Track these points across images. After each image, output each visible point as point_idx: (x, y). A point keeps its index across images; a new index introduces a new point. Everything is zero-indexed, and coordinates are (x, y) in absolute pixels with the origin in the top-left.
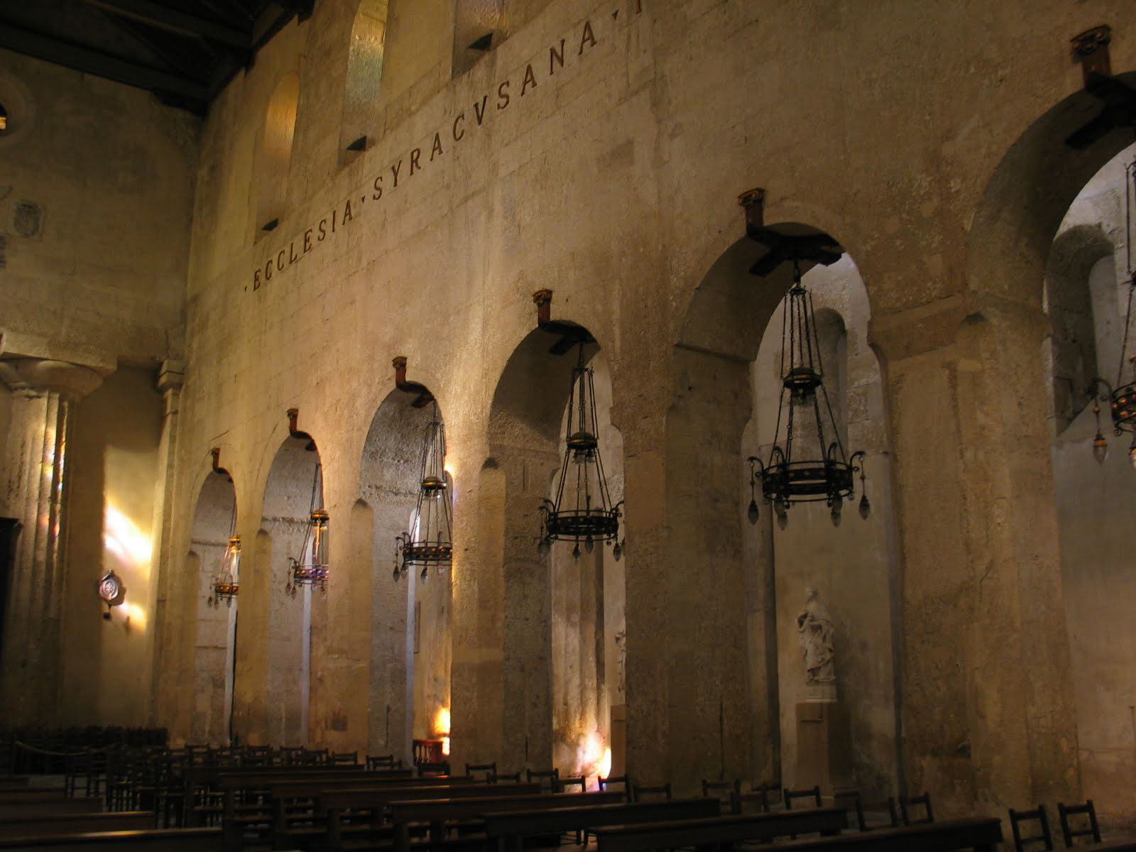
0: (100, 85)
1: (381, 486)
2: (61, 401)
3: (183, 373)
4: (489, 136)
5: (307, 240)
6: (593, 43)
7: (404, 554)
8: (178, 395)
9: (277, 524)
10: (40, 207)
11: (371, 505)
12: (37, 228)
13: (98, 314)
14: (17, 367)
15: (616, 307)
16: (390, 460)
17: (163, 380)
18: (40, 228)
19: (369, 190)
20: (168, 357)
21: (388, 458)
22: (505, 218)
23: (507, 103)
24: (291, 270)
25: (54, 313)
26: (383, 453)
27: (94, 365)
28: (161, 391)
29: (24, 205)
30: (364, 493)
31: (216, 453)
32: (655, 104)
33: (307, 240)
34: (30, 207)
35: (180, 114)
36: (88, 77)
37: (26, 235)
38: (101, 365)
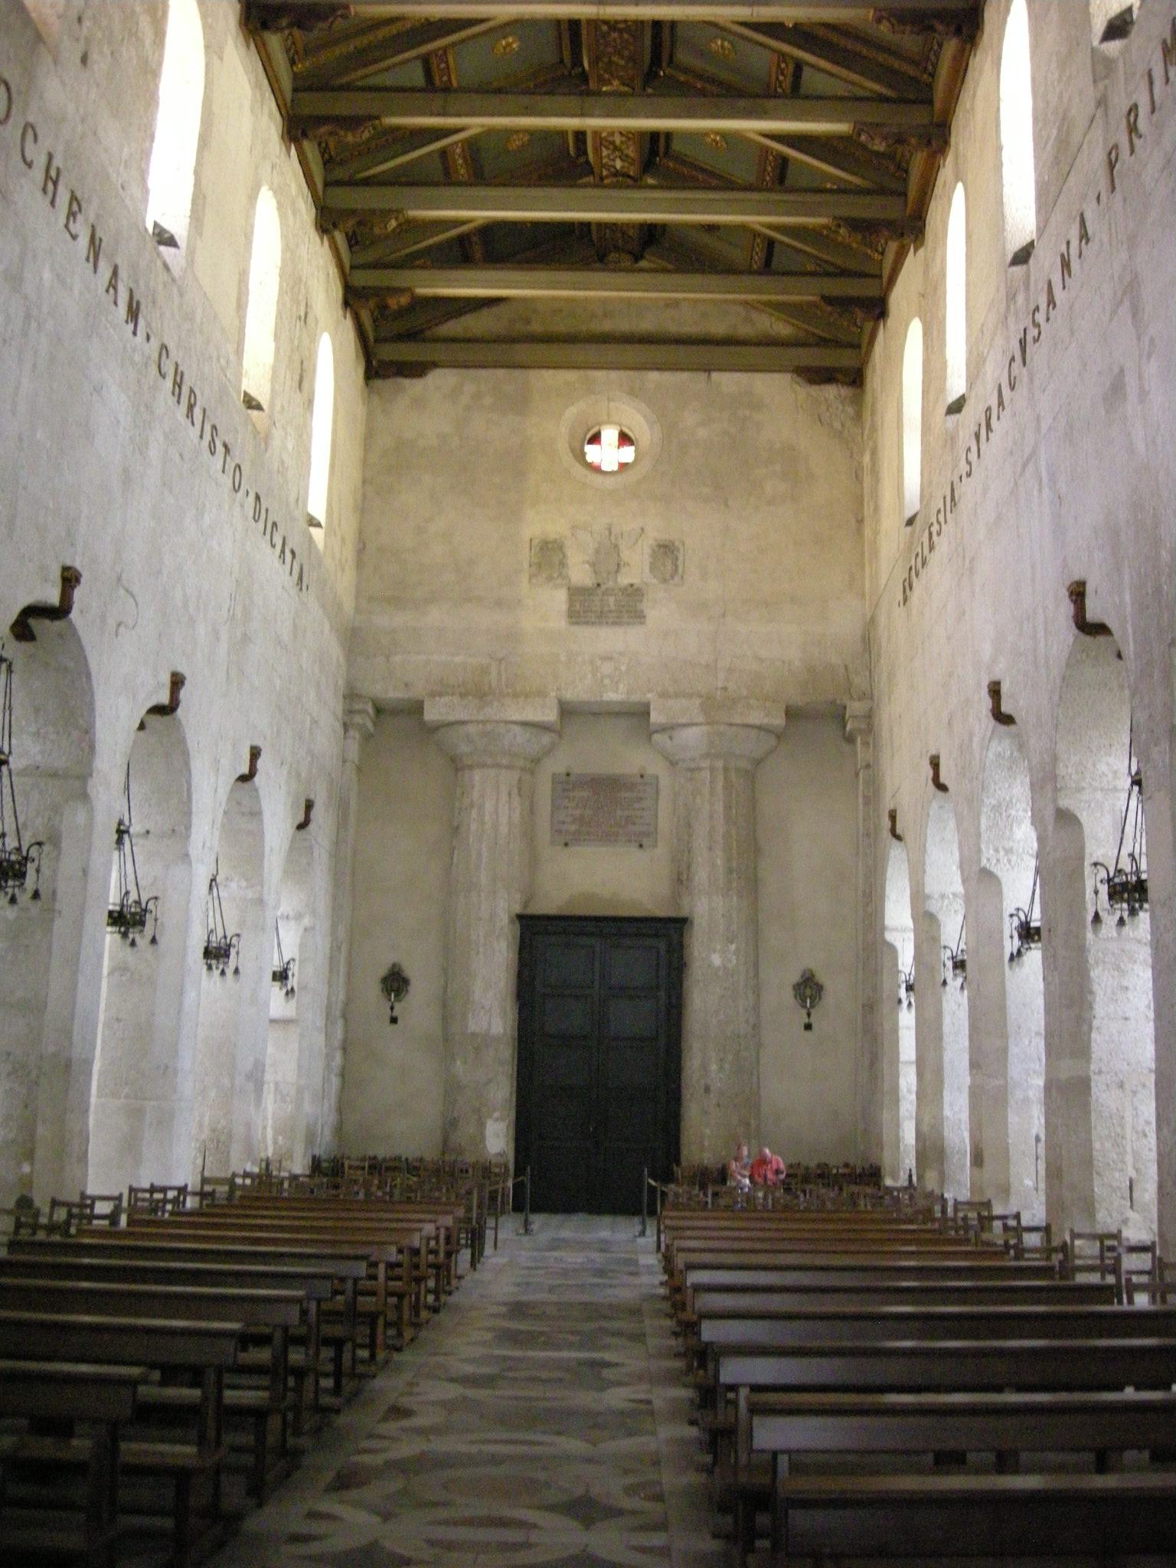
0: (728, 382)
1: (1012, 848)
2: (726, 769)
3: (869, 716)
4: (1031, 380)
5: (930, 534)
6: (1087, 243)
7: (1020, 937)
8: (868, 743)
9: (946, 901)
10: (677, 543)
11: (999, 874)
12: (676, 567)
13: (761, 660)
14: (671, 738)
15: (1127, 598)
16: (1021, 813)
17: (849, 727)
18: (680, 570)
19: (964, 468)
20: (852, 698)
21: (1017, 811)
22: (1050, 488)
23: (1040, 333)
24: (923, 573)
25: (707, 666)
26: (1010, 804)
27: (757, 722)
28: (850, 739)
29: (659, 546)
30: (988, 860)
31: (893, 817)
32: (1135, 314)
33: (930, 534)
34: (665, 546)
35: (831, 392)
36: (715, 375)
37: (665, 581)
38: (766, 721)
